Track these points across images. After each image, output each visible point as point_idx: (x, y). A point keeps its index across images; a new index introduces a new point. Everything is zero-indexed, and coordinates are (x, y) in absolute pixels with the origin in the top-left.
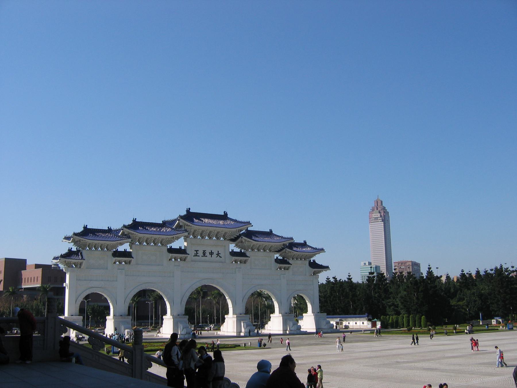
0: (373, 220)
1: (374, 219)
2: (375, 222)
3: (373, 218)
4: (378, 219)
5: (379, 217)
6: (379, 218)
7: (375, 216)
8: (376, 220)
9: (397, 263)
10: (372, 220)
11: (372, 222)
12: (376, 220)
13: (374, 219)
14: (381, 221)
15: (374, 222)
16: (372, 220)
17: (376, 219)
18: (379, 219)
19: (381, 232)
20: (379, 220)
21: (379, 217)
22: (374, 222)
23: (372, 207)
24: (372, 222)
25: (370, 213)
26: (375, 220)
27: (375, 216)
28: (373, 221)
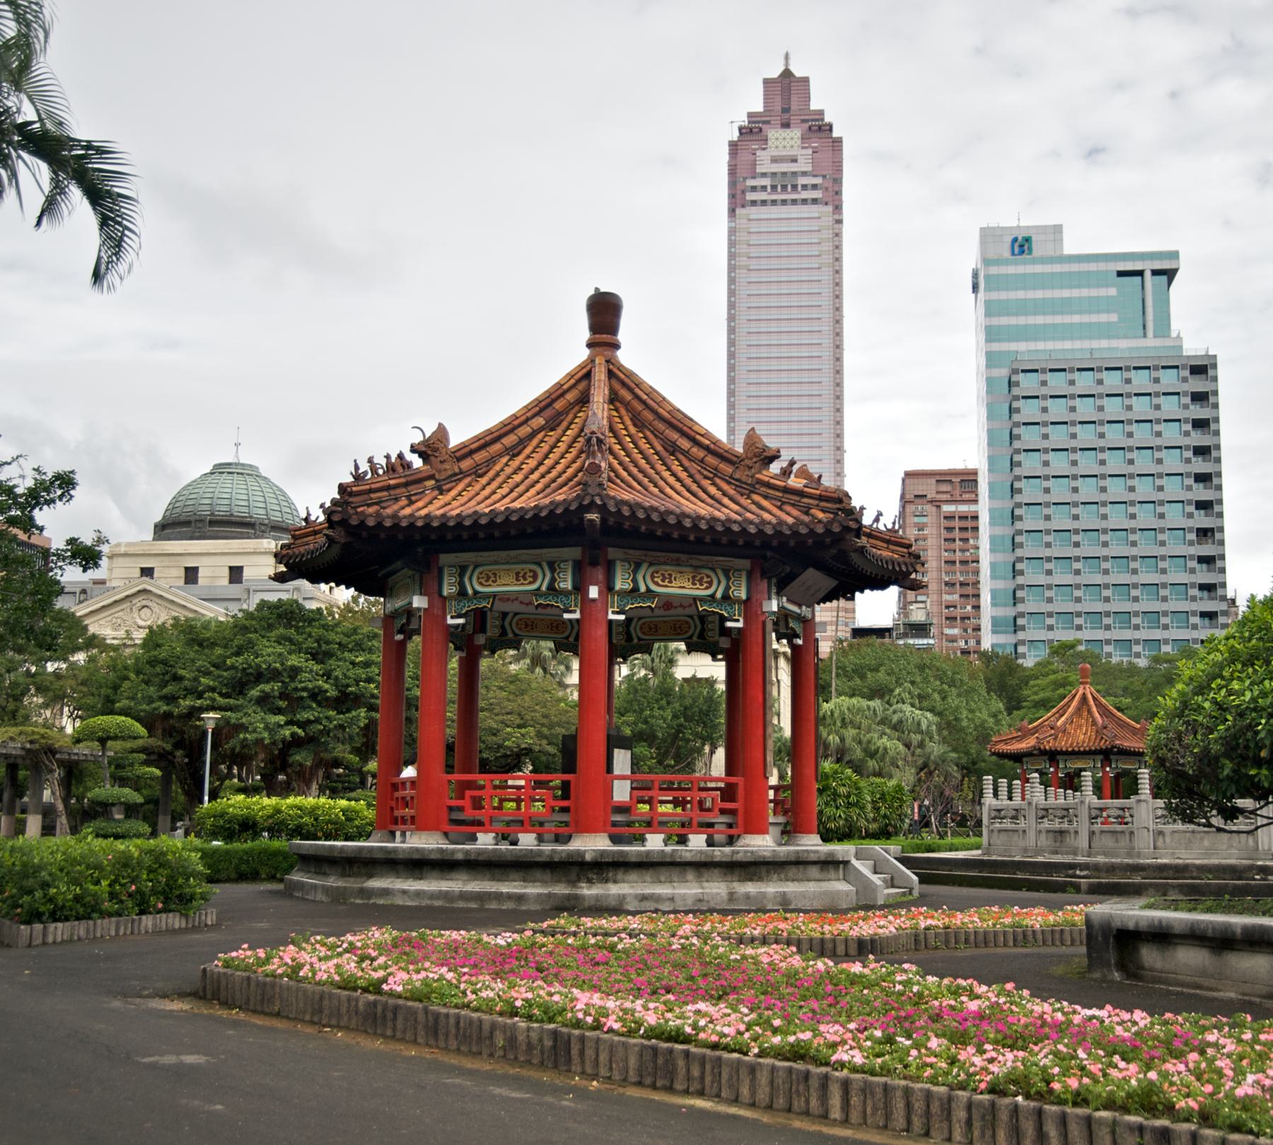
0: (764, 188)
1: (766, 182)
2: (774, 202)
3: (764, 175)
4: (794, 187)
5: (804, 174)
6: (802, 181)
7: (775, 160)
8: (784, 187)
9: (933, 481)
10: (754, 189)
11: (754, 203)
13: (766, 182)
15: (764, 203)
16: (754, 189)
17: (785, 182)
18: (805, 187)
21: (804, 174)
22: (764, 203)
23: (750, 115)
24: (754, 203)
25: (733, 146)
26: (774, 187)
27: (775, 160)
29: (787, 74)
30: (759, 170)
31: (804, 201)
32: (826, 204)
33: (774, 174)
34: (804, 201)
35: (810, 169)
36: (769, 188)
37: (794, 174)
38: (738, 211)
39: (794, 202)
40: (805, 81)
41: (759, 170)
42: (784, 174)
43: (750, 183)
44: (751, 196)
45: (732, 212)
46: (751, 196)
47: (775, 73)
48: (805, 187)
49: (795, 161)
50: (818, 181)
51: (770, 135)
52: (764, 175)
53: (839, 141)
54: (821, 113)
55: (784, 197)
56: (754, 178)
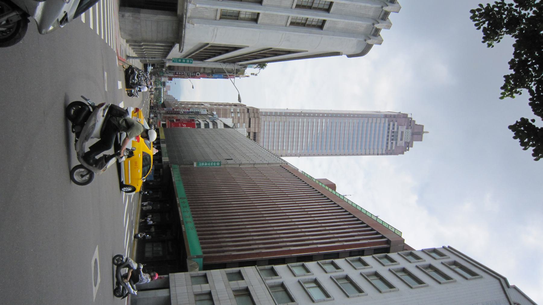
0: (393, 129)
1: (395, 130)
2: (388, 132)
3: (398, 129)
4: (393, 140)
5: (396, 143)
6: (394, 142)
7: (402, 132)
8: (393, 136)
10: (394, 125)
11: (389, 125)
12: (393, 136)
14: (387, 147)
15: (389, 129)
16: (394, 125)
18: (392, 143)
19: (363, 147)
20: (390, 143)
21: (396, 143)
22: (389, 129)
23: (414, 121)
24: (389, 125)
25: (405, 116)
26: (393, 132)
27: (402, 132)
28: (391, 129)
29: (424, 132)
30: (400, 127)
31: (387, 143)
32: (385, 150)
33: (397, 132)
34: (387, 143)
35: (398, 145)
36: (393, 130)
37: (397, 140)
38: (387, 119)
39: (388, 140)
40: (421, 140)
41: (400, 127)
42: (397, 136)
43: (396, 124)
44: (391, 124)
45: (386, 116)
46: (391, 124)
47: (425, 130)
48: (392, 143)
49: (401, 140)
50: (394, 148)
51: (409, 130)
52: (398, 129)
53: (403, 153)
54: (412, 147)
55: (390, 136)
56: (398, 125)
